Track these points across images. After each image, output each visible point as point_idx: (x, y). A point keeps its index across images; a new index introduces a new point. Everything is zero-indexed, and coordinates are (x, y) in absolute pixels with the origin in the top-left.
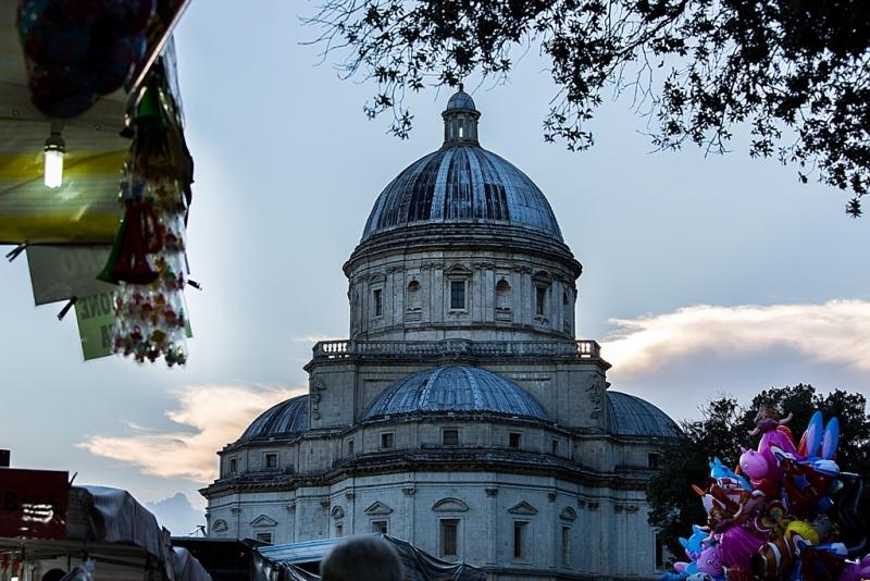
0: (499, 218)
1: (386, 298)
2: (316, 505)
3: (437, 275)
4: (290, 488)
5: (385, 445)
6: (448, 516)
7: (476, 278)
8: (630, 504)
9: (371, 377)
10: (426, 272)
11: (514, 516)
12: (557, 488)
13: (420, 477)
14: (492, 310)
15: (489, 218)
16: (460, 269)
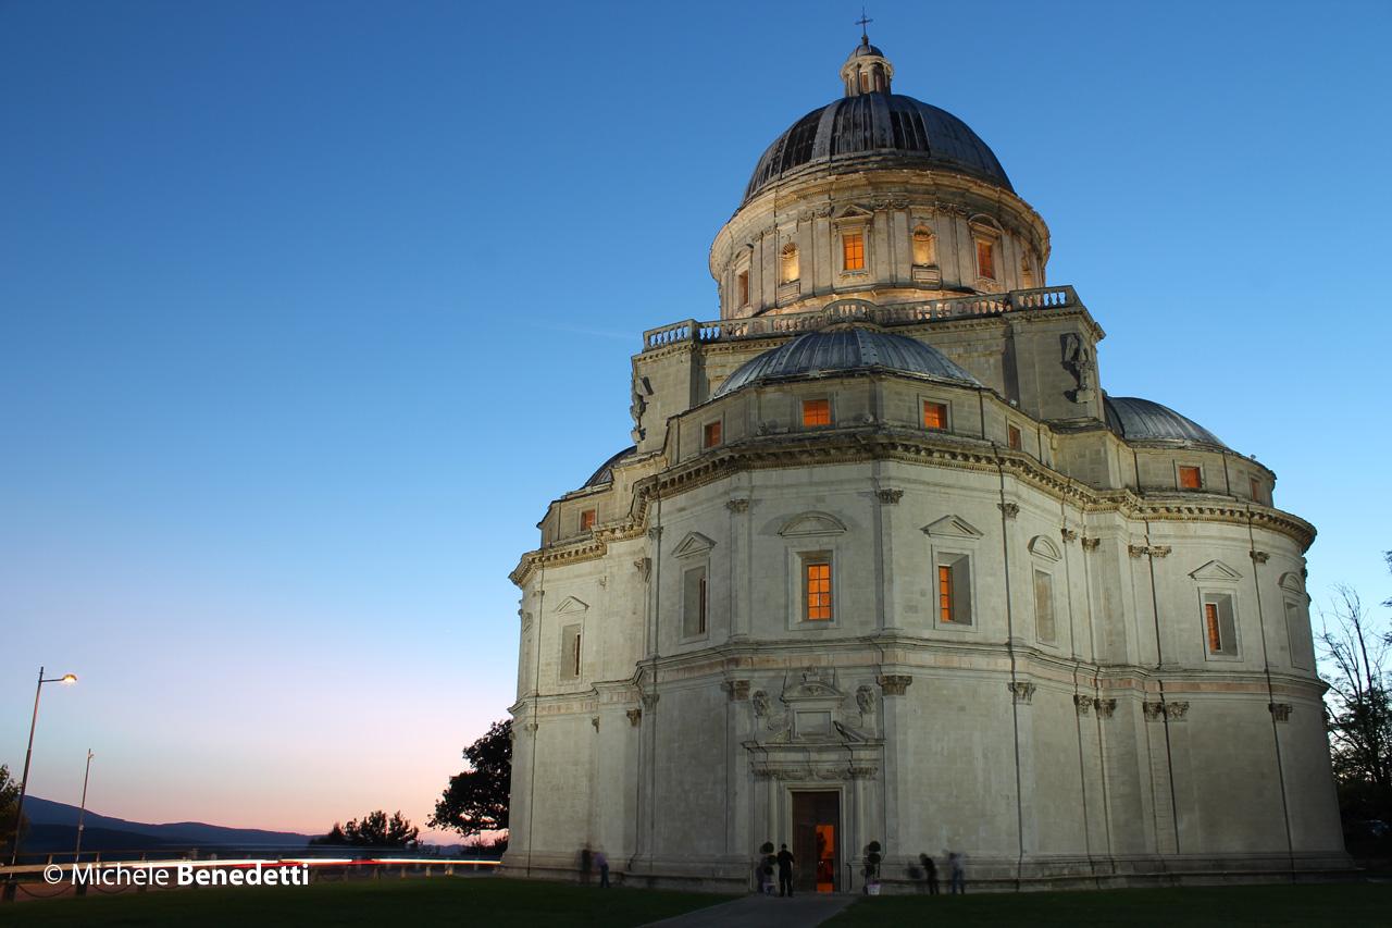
0: (913, 147)
1: (754, 282)
2: (629, 567)
3: (820, 227)
4: (599, 551)
5: (709, 442)
6: (812, 546)
7: (880, 223)
8: (1154, 542)
9: (719, 371)
10: (805, 225)
11: (936, 541)
12: (1019, 497)
13: (759, 476)
14: (907, 267)
15: (898, 147)
16: (854, 214)
